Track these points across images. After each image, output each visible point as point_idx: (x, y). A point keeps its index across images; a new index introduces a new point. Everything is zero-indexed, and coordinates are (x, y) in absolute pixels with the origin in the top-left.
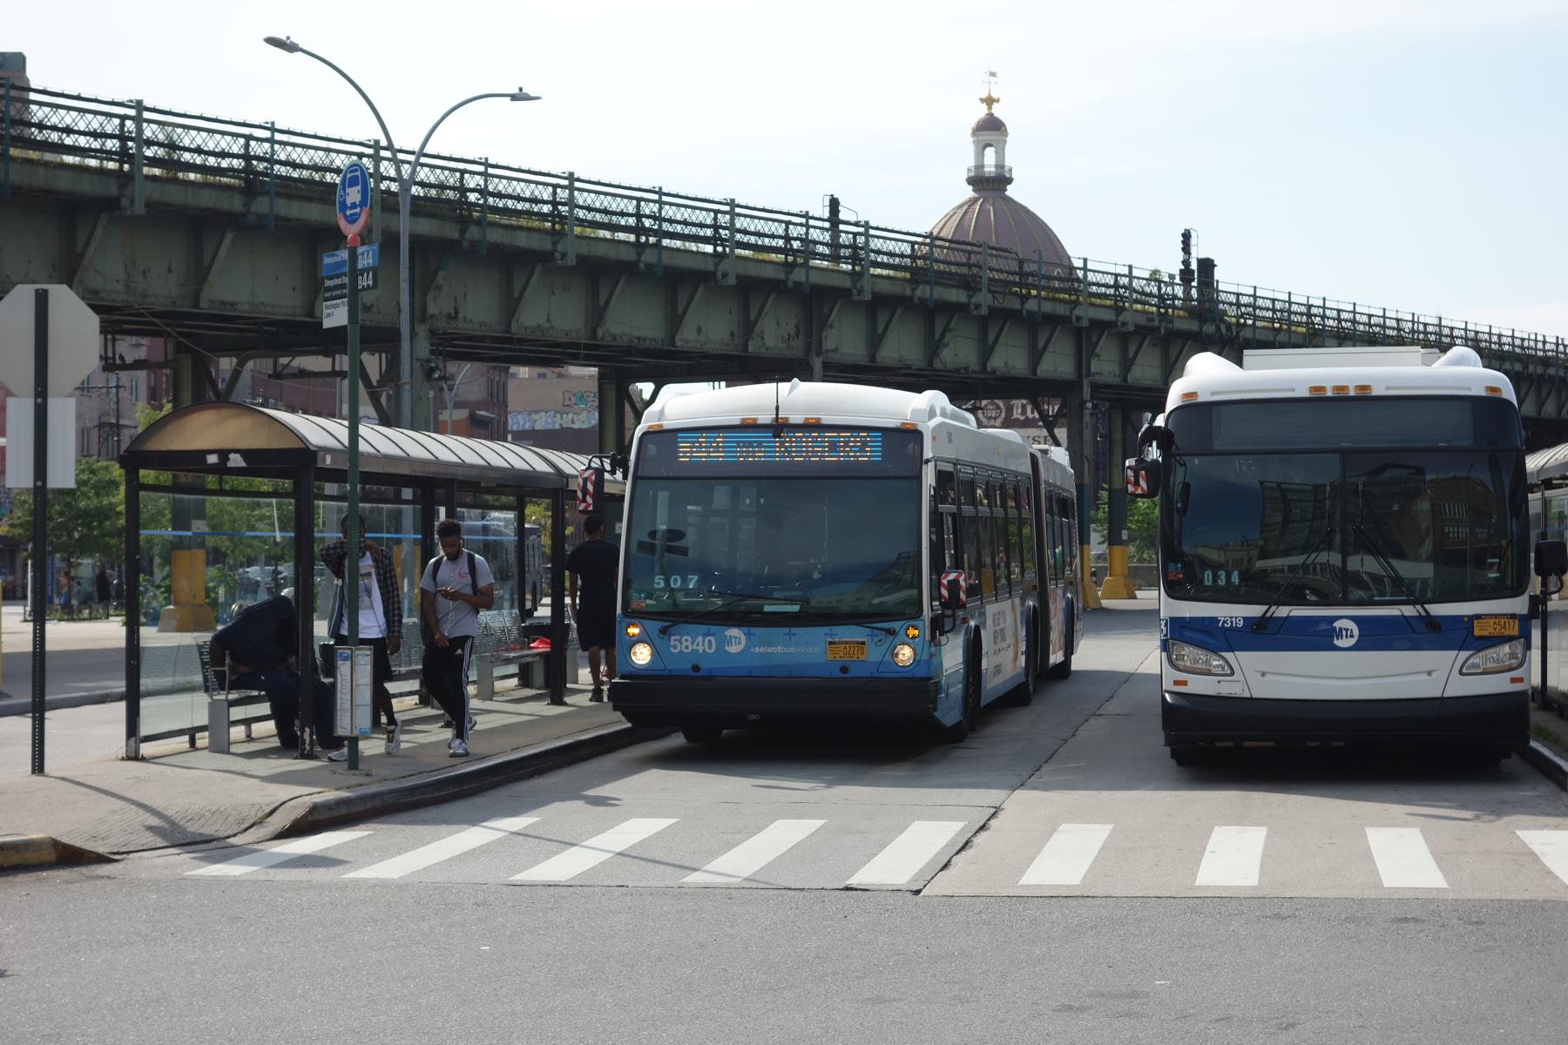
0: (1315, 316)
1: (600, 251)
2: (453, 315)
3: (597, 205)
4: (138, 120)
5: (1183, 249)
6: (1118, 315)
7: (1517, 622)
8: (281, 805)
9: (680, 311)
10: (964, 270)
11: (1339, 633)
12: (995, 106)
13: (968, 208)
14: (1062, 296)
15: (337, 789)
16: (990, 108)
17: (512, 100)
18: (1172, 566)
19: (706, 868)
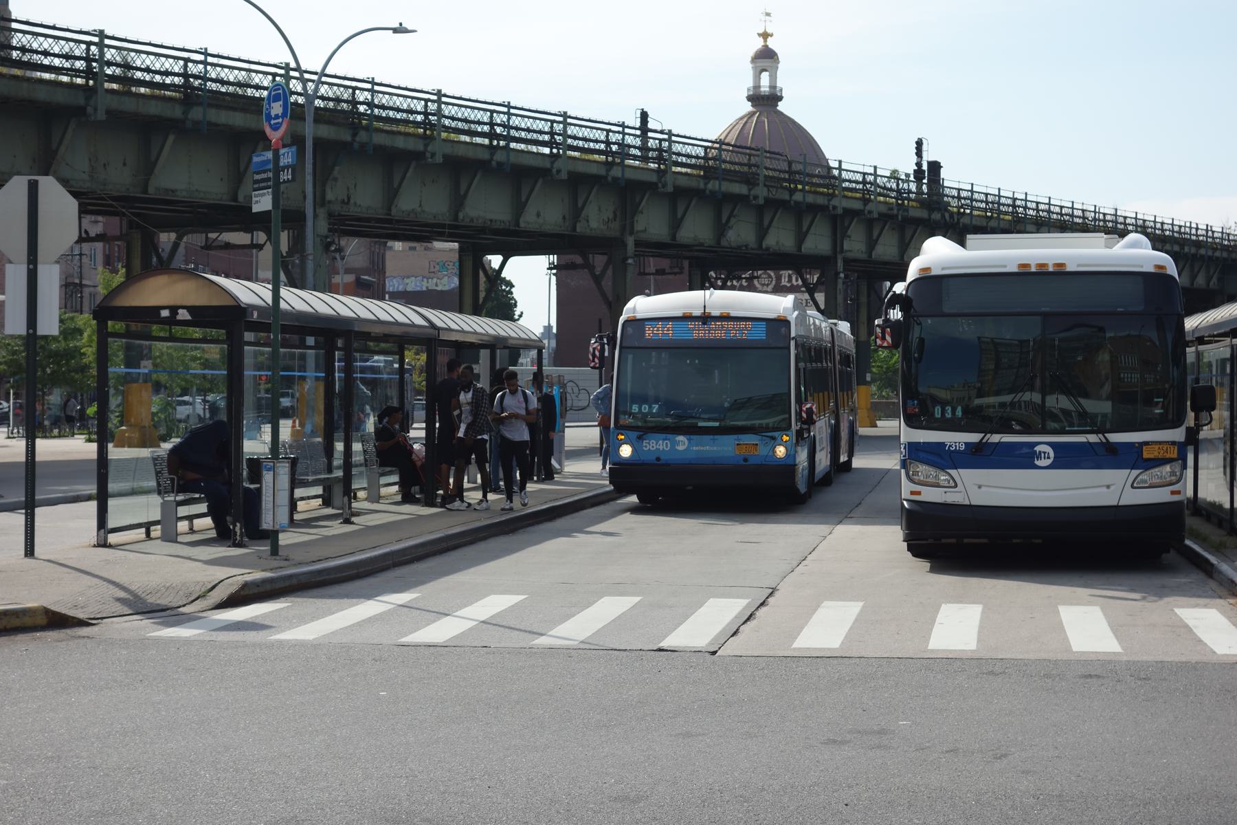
0: (1019, 207)
1: (461, 151)
2: (346, 200)
3: (460, 115)
4: (101, 45)
5: (917, 154)
6: (865, 205)
7: (1176, 447)
8: (219, 583)
9: (523, 199)
10: (746, 169)
11: (1039, 456)
12: (769, 39)
13: (747, 120)
14: (821, 190)
15: (263, 571)
16: (765, 41)
17: (394, 33)
18: (910, 402)
19: (550, 633)
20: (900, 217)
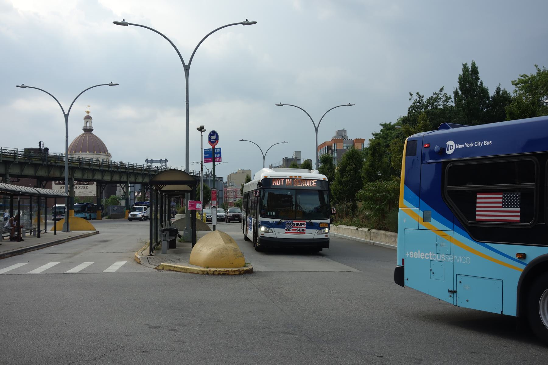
5: (39, 145)
6: (15, 160)
12: (89, 113)
20: (30, 163)
